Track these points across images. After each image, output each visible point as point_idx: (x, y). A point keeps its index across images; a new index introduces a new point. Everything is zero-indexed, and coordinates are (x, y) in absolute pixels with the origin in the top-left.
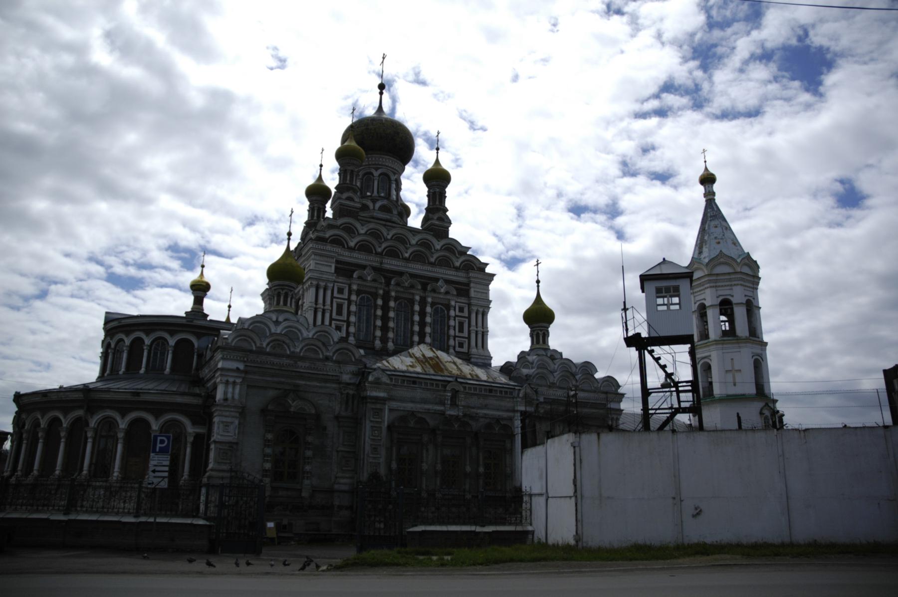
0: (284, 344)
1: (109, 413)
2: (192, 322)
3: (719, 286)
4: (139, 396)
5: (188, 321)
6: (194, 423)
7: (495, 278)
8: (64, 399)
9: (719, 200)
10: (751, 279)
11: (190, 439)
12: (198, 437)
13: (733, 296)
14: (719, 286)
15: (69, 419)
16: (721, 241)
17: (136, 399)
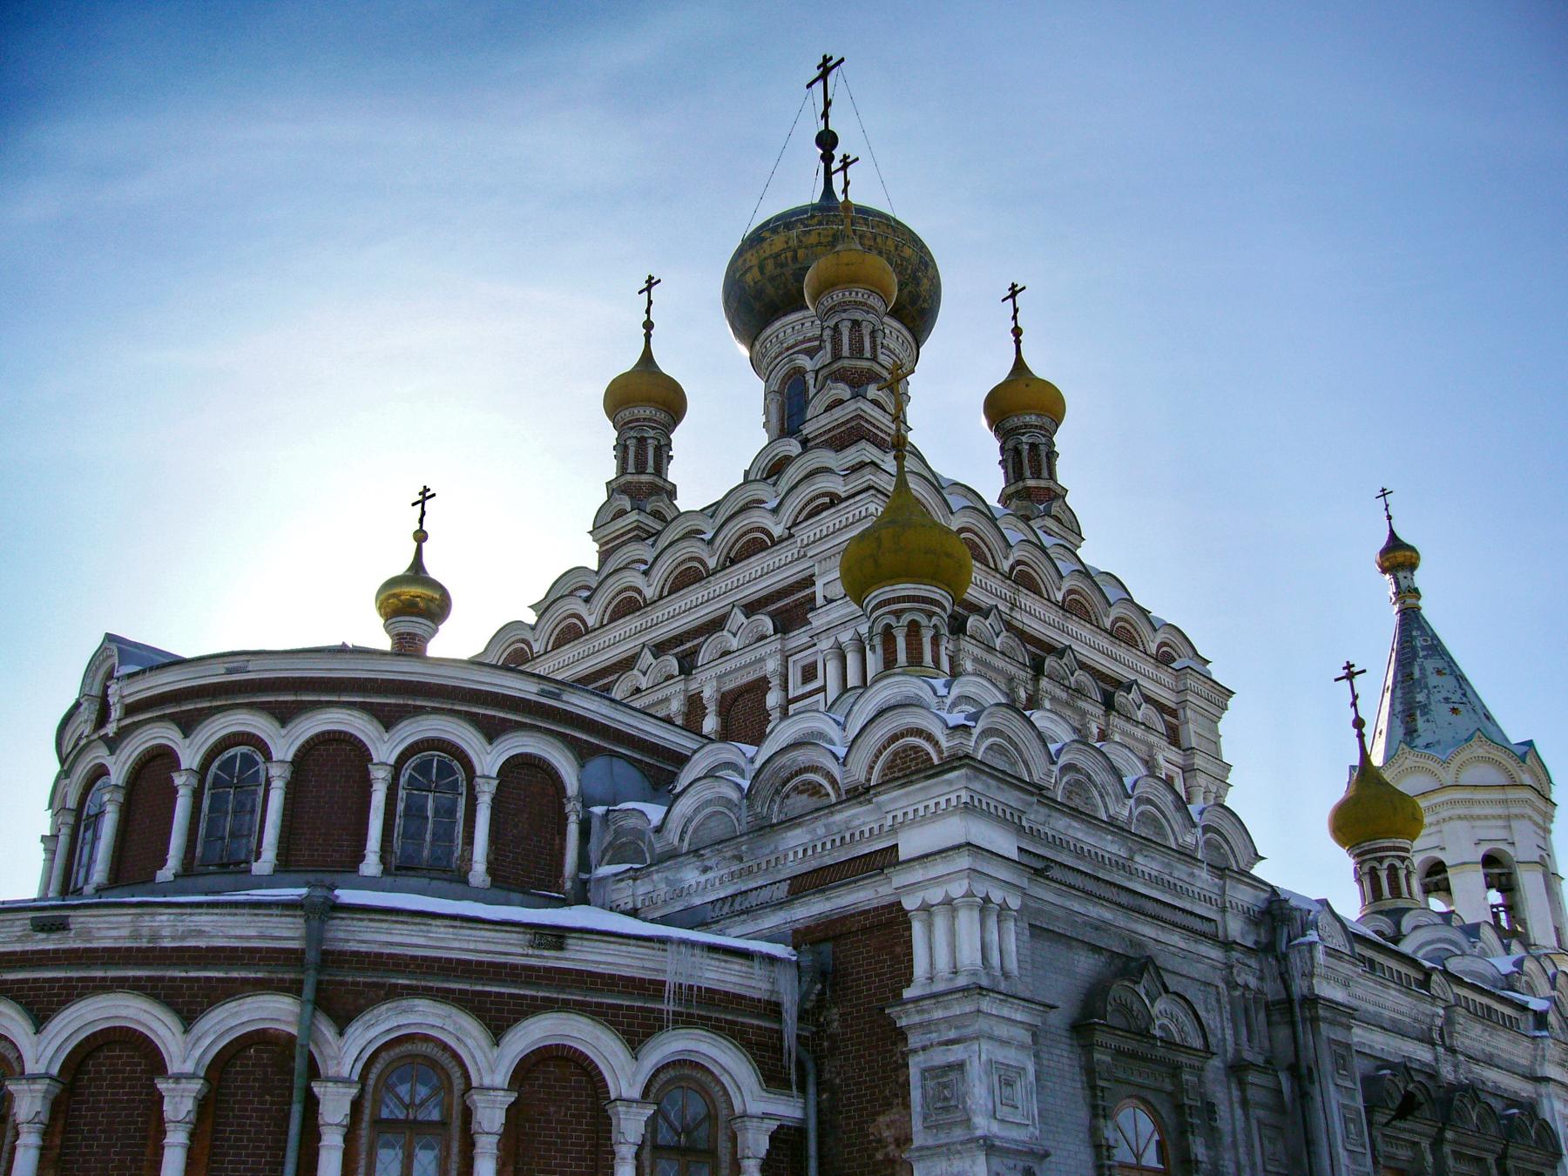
0: (1089, 784)
1: (425, 1016)
2: (557, 697)
3: (1479, 818)
4: (560, 947)
5: (542, 693)
6: (773, 1079)
7: (1231, 702)
8: (167, 943)
9: (1429, 609)
10: (1540, 803)
11: (756, 1142)
12: (786, 1140)
13: (1443, 849)
14: (1479, 818)
15: (207, 1042)
16: (1460, 707)
17: (550, 959)
